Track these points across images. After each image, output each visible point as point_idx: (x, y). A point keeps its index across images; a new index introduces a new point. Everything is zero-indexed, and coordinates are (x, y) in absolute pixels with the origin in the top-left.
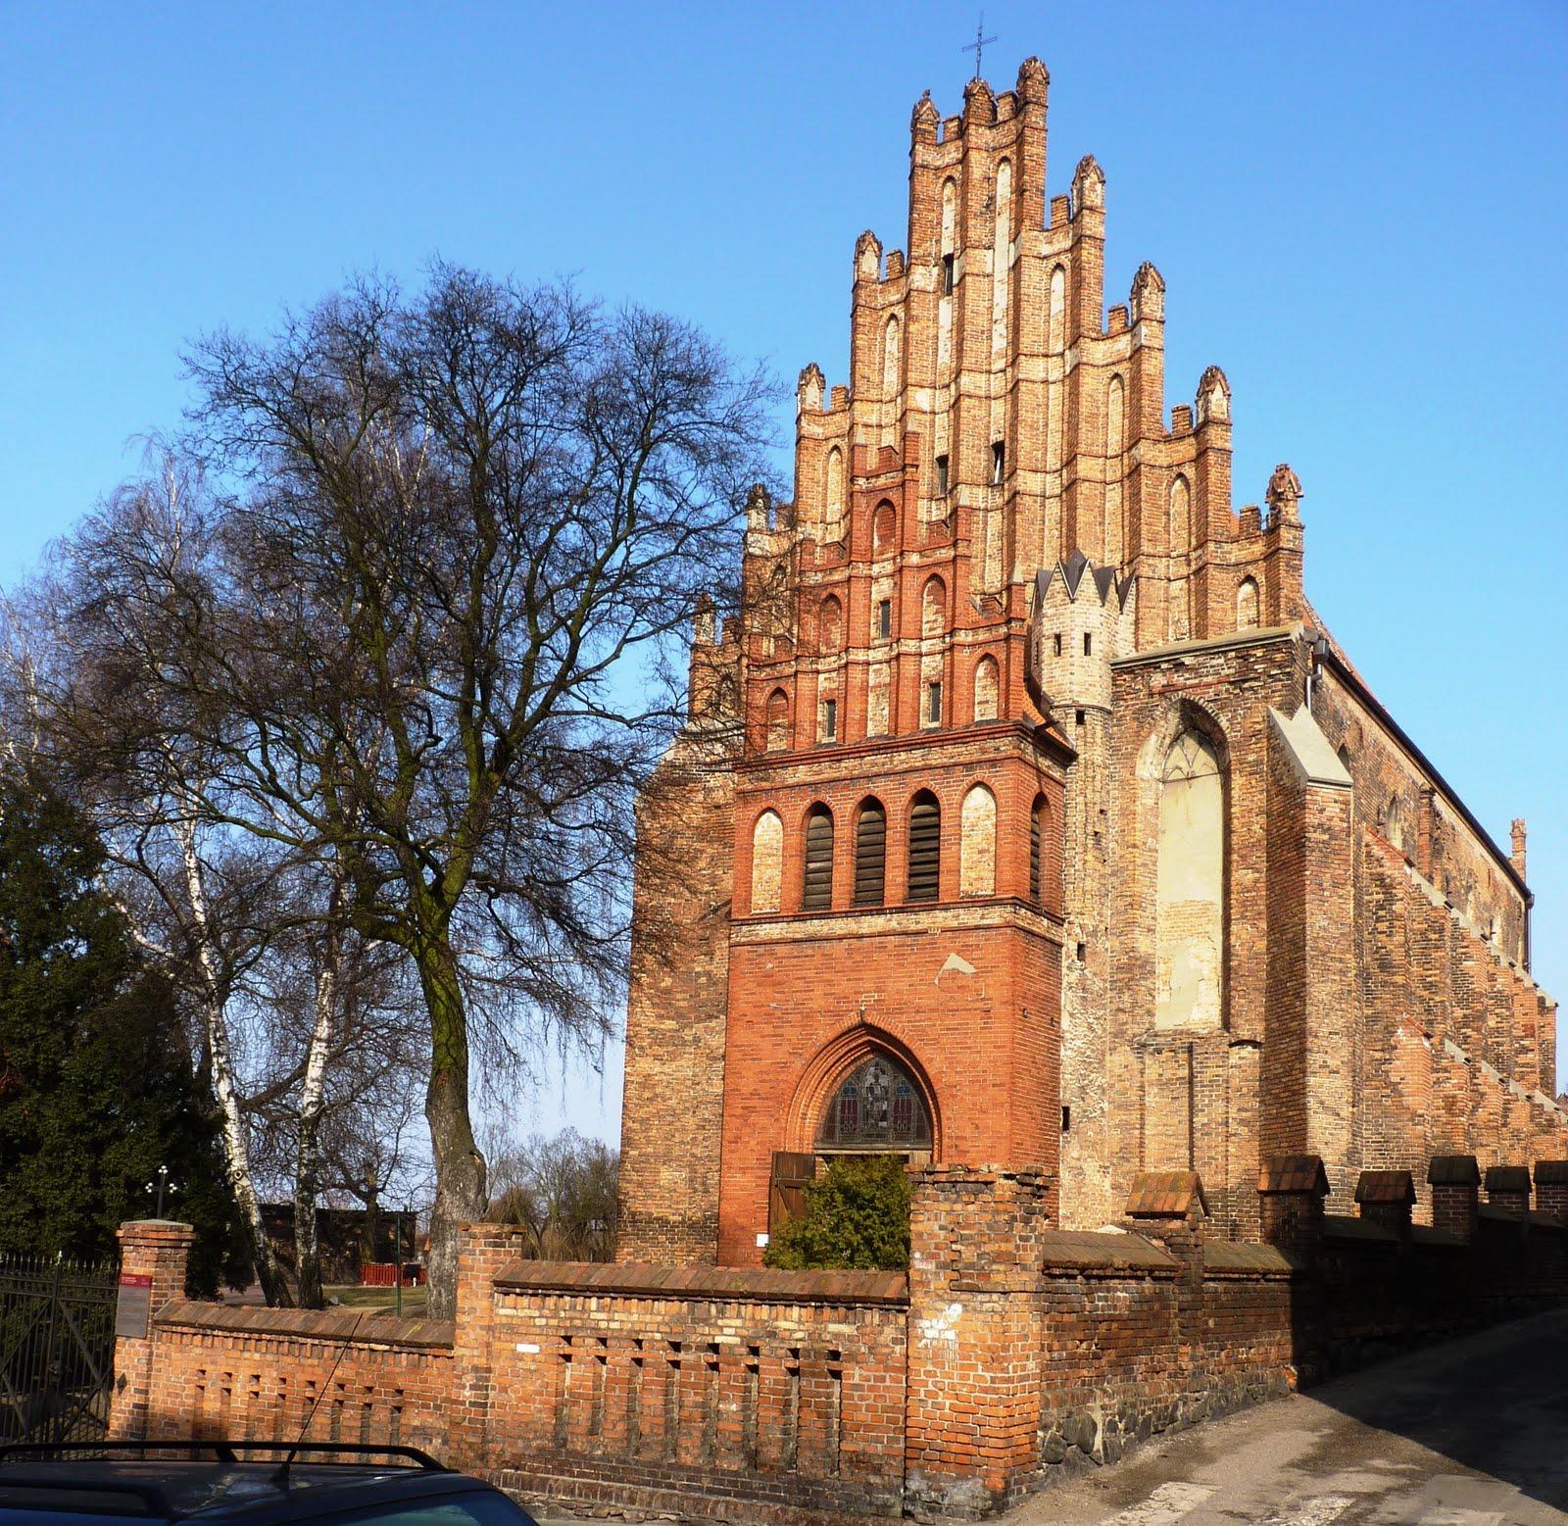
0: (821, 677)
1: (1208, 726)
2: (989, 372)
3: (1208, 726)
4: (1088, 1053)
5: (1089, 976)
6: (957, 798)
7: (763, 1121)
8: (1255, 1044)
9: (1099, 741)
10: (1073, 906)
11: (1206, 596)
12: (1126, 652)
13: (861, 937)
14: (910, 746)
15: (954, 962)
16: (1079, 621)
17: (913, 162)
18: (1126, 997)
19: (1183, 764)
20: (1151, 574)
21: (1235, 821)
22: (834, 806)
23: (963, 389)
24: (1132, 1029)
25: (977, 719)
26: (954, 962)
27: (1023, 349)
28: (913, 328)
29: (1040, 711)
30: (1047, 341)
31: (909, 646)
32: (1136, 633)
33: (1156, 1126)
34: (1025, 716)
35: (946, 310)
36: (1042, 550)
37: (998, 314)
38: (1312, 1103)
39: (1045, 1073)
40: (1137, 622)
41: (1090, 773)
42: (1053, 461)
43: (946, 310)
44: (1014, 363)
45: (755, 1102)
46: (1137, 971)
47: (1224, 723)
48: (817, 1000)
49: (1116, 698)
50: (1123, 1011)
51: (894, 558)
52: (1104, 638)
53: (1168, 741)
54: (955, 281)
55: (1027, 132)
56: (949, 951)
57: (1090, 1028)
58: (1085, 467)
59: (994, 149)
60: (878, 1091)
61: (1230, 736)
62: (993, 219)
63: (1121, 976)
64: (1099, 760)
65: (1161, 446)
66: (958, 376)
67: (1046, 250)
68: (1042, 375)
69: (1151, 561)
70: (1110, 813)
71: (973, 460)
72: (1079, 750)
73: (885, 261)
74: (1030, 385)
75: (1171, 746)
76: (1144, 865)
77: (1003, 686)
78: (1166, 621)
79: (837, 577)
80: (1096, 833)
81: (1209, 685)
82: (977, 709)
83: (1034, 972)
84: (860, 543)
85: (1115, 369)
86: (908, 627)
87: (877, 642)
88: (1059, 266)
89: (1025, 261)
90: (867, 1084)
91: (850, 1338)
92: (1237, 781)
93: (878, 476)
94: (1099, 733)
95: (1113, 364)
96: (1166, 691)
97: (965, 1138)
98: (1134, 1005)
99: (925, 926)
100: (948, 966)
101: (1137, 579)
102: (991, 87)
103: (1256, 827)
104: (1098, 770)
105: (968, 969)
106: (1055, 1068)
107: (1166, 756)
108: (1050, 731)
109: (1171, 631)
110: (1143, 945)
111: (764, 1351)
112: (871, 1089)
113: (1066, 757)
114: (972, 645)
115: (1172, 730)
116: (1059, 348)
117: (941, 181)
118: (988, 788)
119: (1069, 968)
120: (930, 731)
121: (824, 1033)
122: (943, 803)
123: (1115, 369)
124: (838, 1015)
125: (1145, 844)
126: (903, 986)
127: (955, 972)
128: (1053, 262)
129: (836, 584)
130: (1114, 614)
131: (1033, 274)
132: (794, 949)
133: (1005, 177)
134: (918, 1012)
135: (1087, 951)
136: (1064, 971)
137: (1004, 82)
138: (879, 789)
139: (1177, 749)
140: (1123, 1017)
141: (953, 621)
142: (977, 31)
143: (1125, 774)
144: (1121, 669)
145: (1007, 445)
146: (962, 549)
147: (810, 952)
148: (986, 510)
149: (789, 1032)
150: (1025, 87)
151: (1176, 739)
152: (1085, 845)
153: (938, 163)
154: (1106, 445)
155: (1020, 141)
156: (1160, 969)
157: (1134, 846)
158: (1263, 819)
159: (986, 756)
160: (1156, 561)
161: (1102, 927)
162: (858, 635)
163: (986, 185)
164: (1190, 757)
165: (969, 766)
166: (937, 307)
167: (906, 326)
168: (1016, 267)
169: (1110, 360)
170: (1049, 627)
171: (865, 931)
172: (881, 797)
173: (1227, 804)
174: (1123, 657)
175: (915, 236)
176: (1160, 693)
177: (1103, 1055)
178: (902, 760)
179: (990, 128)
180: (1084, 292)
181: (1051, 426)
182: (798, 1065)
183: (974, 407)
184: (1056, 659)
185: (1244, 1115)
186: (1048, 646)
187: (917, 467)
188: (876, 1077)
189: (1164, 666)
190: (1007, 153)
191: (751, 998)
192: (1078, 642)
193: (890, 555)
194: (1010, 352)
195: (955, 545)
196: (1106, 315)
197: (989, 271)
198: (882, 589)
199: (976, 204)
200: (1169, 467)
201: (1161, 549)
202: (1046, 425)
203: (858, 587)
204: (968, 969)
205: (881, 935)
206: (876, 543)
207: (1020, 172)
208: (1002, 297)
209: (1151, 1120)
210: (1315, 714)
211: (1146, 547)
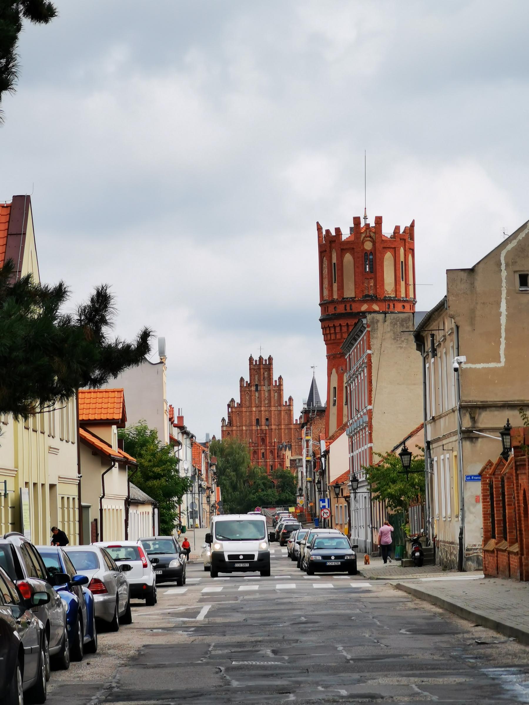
35: (257, 394)
43: (257, 394)
58: (283, 427)
67: (274, 389)
116: (277, 405)
133: (266, 373)
137: (265, 357)
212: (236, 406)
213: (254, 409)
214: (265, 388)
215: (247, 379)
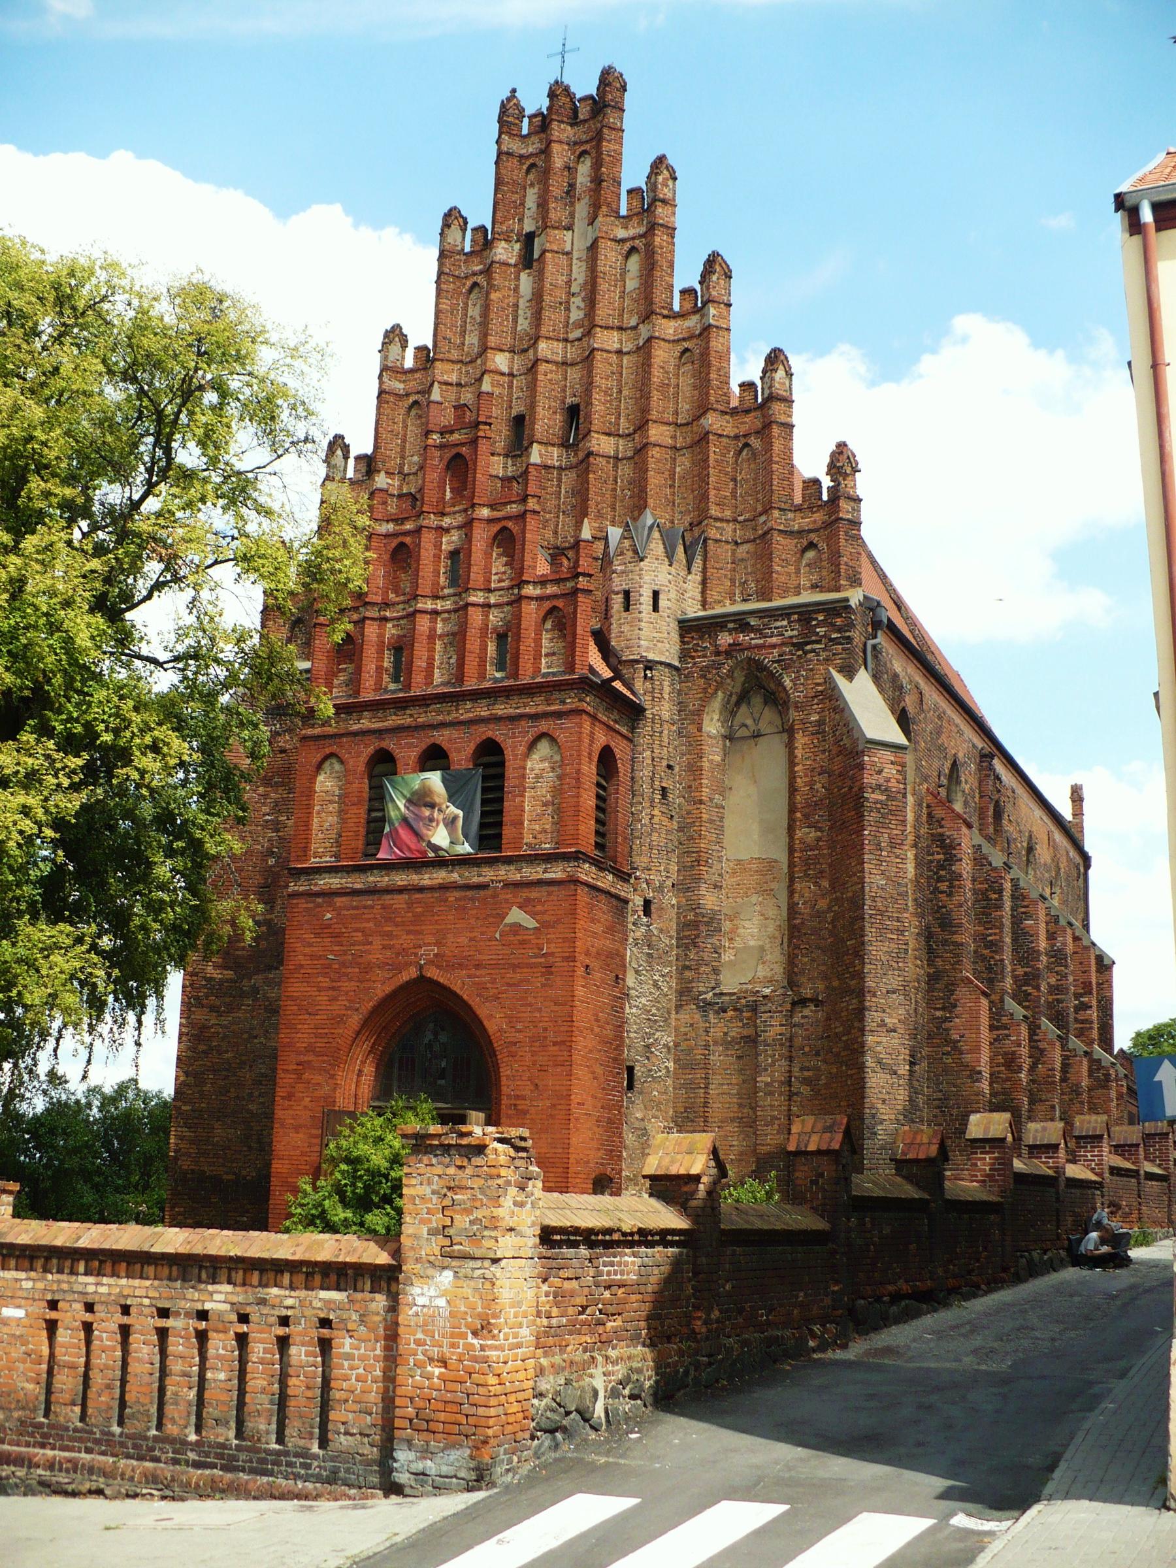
0: (389, 625)
1: (772, 685)
2: (566, 340)
3: (772, 685)
4: (654, 1011)
6: (522, 749)
7: (318, 1078)
9: (666, 696)
10: (641, 861)
11: (771, 560)
12: (694, 611)
13: (421, 889)
14: (476, 695)
15: (516, 915)
16: (647, 578)
17: (499, 149)
19: (749, 722)
20: (718, 536)
21: (799, 780)
22: (399, 754)
23: (540, 355)
25: (543, 671)
26: (516, 915)
27: (599, 320)
28: (494, 296)
29: (608, 665)
30: (621, 315)
31: (477, 598)
32: (703, 592)
34: (592, 669)
35: (526, 281)
36: (614, 509)
37: (575, 288)
39: (609, 1032)
40: (704, 582)
41: (657, 728)
42: (624, 426)
43: (526, 281)
44: (588, 333)
45: (311, 1057)
46: (703, 928)
47: (787, 683)
48: (376, 953)
49: (684, 655)
50: (688, 968)
51: (466, 510)
52: (673, 595)
53: (734, 699)
54: (536, 256)
55: (605, 131)
56: (513, 904)
57: (656, 985)
58: (656, 433)
59: (575, 143)
60: (437, 1048)
61: (796, 696)
62: (572, 204)
64: (666, 716)
65: (727, 417)
66: (535, 342)
67: (621, 233)
68: (616, 346)
69: (718, 524)
70: (677, 769)
71: (547, 421)
72: (647, 705)
73: (469, 234)
74: (605, 355)
75: (738, 704)
76: (711, 821)
77: (569, 639)
78: (733, 581)
79: (408, 526)
80: (663, 789)
81: (773, 646)
82: (543, 661)
83: (599, 928)
84: (431, 496)
85: (686, 345)
86: (476, 576)
87: (446, 591)
88: (633, 250)
89: (602, 244)
90: (426, 1041)
91: (339, 1307)
92: (801, 740)
93: (452, 432)
94: (667, 689)
95: (684, 339)
96: (735, 647)
97: (523, 1098)
99: (487, 879)
100: (509, 920)
101: (705, 540)
102: (572, 89)
103: (818, 786)
104: (666, 726)
105: (530, 923)
106: (620, 1027)
107: (733, 714)
108: (617, 684)
109: (737, 592)
110: (709, 900)
111: (253, 1318)
112: (430, 1046)
113: (633, 712)
114: (539, 599)
115: (738, 689)
116: (633, 322)
117: (525, 167)
118: (553, 740)
119: (634, 924)
120: (496, 680)
121: (381, 989)
122: (508, 754)
123: (686, 345)
124: (400, 968)
125: (711, 800)
126: (463, 940)
127: (517, 928)
128: (628, 245)
129: (406, 533)
130: (683, 573)
131: (610, 256)
132: (356, 901)
133: (584, 170)
134: (478, 966)
135: (653, 907)
136: (630, 926)
137: (584, 85)
138: (442, 737)
139: (744, 708)
140: (689, 974)
141: (521, 573)
142: (562, 42)
143: (693, 729)
144: (688, 628)
145: (582, 407)
146: (532, 504)
147: (370, 903)
148: (560, 468)
149: (347, 985)
150: (605, 92)
151: (743, 698)
152: (652, 801)
153: (523, 151)
154: (676, 413)
155: (598, 138)
156: (727, 926)
157: (701, 802)
158: (824, 779)
159: (553, 708)
160: (725, 525)
161: (669, 883)
162: (425, 587)
163: (566, 173)
164: (757, 716)
165: (535, 717)
166: (518, 278)
167: (488, 293)
168: (593, 247)
169: (681, 336)
170: (618, 584)
171: (426, 882)
172: (445, 746)
173: (792, 763)
174: (691, 615)
175: (499, 214)
176: (728, 653)
177: (669, 1013)
178: (466, 711)
179: (572, 125)
180: (657, 274)
181: (625, 393)
182: (355, 1020)
183: (551, 372)
184: (624, 614)
186: (617, 601)
187: (490, 424)
188: (436, 1034)
189: (731, 626)
190: (587, 147)
191: (307, 950)
192: (646, 599)
193: (461, 507)
194: (586, 323)
195: (524, 500)
196: (677, 297)
197: (568, 248)
198: (450, 541)
199: (557, 186)
200: (736, 437)
201: (728, 514)
202: (620, 392)
203: (427, 538)
204: (530, 923)
205: (444, 887)
206: (448, 495)
207: (597, 165)
208: (579, 273)
210: (876, 678)
211: (714, 511)
212: (409, 363)
213: (501, 361)
214: (575, 241)
215: (480, 214)
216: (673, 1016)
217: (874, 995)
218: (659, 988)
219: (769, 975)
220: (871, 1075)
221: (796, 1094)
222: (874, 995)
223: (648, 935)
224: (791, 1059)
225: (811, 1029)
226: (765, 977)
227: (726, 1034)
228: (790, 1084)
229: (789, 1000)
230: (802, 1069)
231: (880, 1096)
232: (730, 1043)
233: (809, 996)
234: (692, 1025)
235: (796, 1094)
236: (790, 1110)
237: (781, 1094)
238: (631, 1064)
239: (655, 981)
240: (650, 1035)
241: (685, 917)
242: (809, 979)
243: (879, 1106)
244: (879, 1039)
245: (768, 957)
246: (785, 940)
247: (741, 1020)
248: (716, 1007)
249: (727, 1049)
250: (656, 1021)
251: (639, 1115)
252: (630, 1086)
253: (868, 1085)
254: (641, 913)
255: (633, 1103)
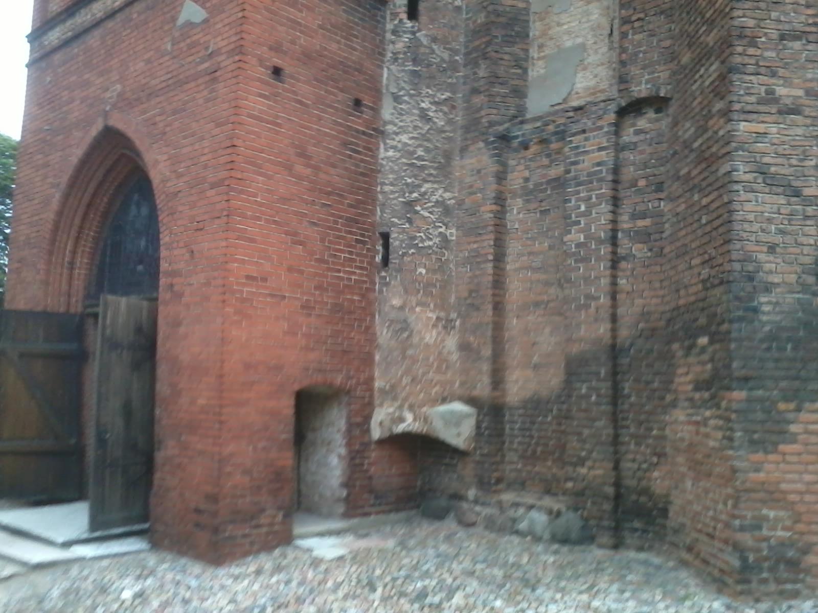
4: (420, 152)
5: (425, 41)
8: (658, 103)
18: (482, 73)
24: (488, 115)
33: (520, 255)
38: (743, 172)
57: (424, 116)
63: (477, 43)
98: (494, 79)
119: (394, 32)
136: (389, 36)
140: (478, 100)
156: (535, 29)
185: (641, 223)
209: (513, 247)
216: (457, 162)
217: (753, 43)
218: (429, 120)
219: (592, 83)
220: (743, 196)
221: (624, 258)
222: (753, 43)
223: (415, 44)
224: (616, 201)
225: (649, 150)
226: (587, 89)
227: (527, 180)
228: (614, 241)
229: (613, 107)
230: (634, 217)
231: (763, 237)
232: (531, 192)
233: (644, 94)
234: (479, 171)
235: (624, 258)
236: (614, 284)
237: (599, 259)
238: (385, 229)
239: (423, 110)
240: (414, 188)
241: (475, 22)
242: (644, 68)
243: (762, 257)
244: (761, 128)
245: (590, 60)
246: (616, 26)
247: (548, 156)
248: (515, 143)
249: (528, 201)
250: (422, 168)
251: (396, 302)
252: (386, 261)
253: (738, 216)
254: (404, 16)
255: (387, 284)
